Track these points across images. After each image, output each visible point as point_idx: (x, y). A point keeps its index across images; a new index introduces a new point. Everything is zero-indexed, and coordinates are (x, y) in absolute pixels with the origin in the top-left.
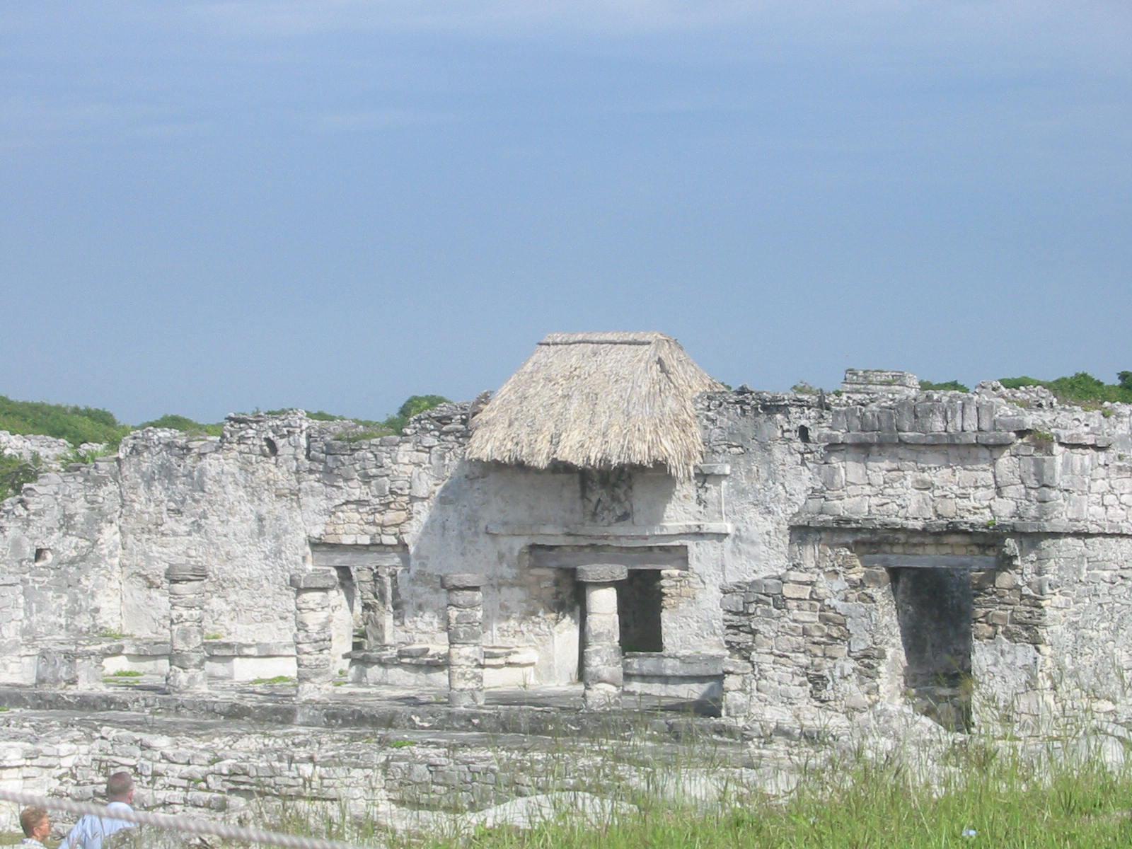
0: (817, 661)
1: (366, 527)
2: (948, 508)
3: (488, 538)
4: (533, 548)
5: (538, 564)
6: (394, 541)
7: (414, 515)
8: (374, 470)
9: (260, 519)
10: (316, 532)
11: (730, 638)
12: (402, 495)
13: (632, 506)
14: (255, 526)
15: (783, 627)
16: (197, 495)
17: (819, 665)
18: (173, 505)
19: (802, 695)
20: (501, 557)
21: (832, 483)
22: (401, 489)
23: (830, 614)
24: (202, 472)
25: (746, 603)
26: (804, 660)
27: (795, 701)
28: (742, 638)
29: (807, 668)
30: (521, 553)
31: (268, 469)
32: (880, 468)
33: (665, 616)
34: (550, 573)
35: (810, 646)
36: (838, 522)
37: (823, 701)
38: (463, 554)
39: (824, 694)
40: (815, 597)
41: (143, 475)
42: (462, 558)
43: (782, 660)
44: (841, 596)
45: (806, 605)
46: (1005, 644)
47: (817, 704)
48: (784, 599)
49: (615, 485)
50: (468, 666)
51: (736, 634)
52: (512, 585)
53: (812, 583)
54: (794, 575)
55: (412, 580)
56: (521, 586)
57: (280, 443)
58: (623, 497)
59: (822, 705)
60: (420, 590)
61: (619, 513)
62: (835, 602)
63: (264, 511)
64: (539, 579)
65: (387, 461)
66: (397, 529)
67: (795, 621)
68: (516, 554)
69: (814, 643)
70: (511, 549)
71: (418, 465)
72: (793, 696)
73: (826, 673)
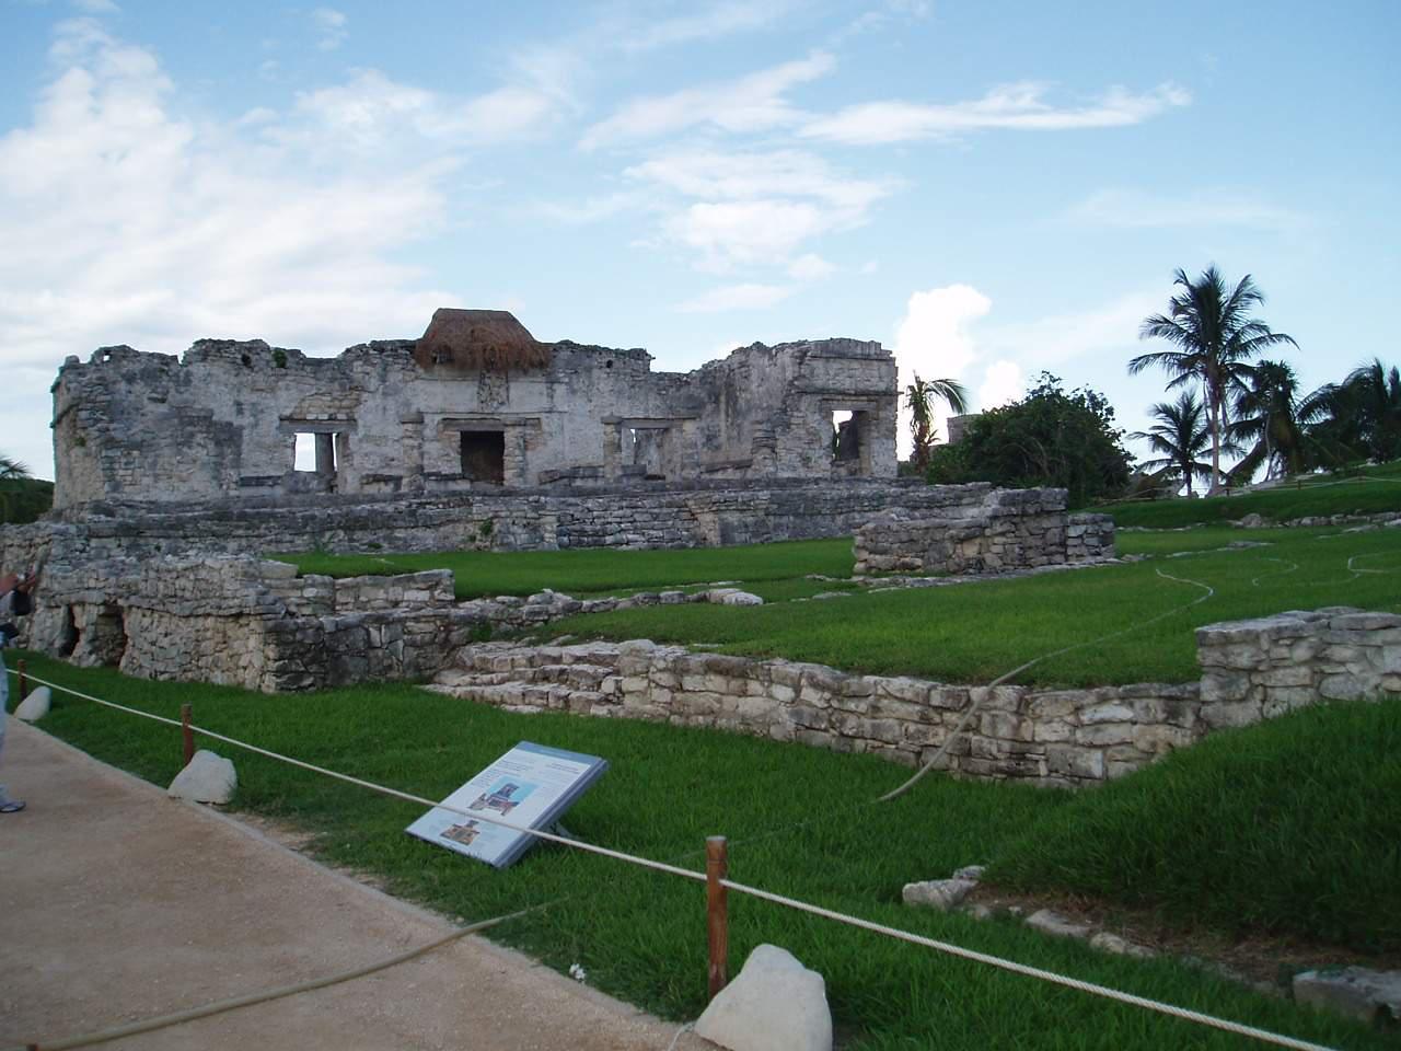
1: (327, 410)
2: (861, 386)
4: (444, 419)
5: (445, 428)
6: (344, 417)
9: (238, 404)
10: (287, 412)
14: (235, 408)
16: (182, 389)
18: (154, 395)
24: (188, 374)
26: (800, 451)
30: (438, 424)
31: (247, 376)
32: (835, 366)
34: (459, 433)
39: (810, 465)
41: (123, 376)
46: (885, 441)
48: (791, 424)
52: (432, 441)
55: (361, 441)
56: (438, 441)
57: (254, 358)
60: (365, 445)
63: (242, 399)
64: (450, 436)
65: (347, 372)
66: (348, 411)
68: (436, 423)
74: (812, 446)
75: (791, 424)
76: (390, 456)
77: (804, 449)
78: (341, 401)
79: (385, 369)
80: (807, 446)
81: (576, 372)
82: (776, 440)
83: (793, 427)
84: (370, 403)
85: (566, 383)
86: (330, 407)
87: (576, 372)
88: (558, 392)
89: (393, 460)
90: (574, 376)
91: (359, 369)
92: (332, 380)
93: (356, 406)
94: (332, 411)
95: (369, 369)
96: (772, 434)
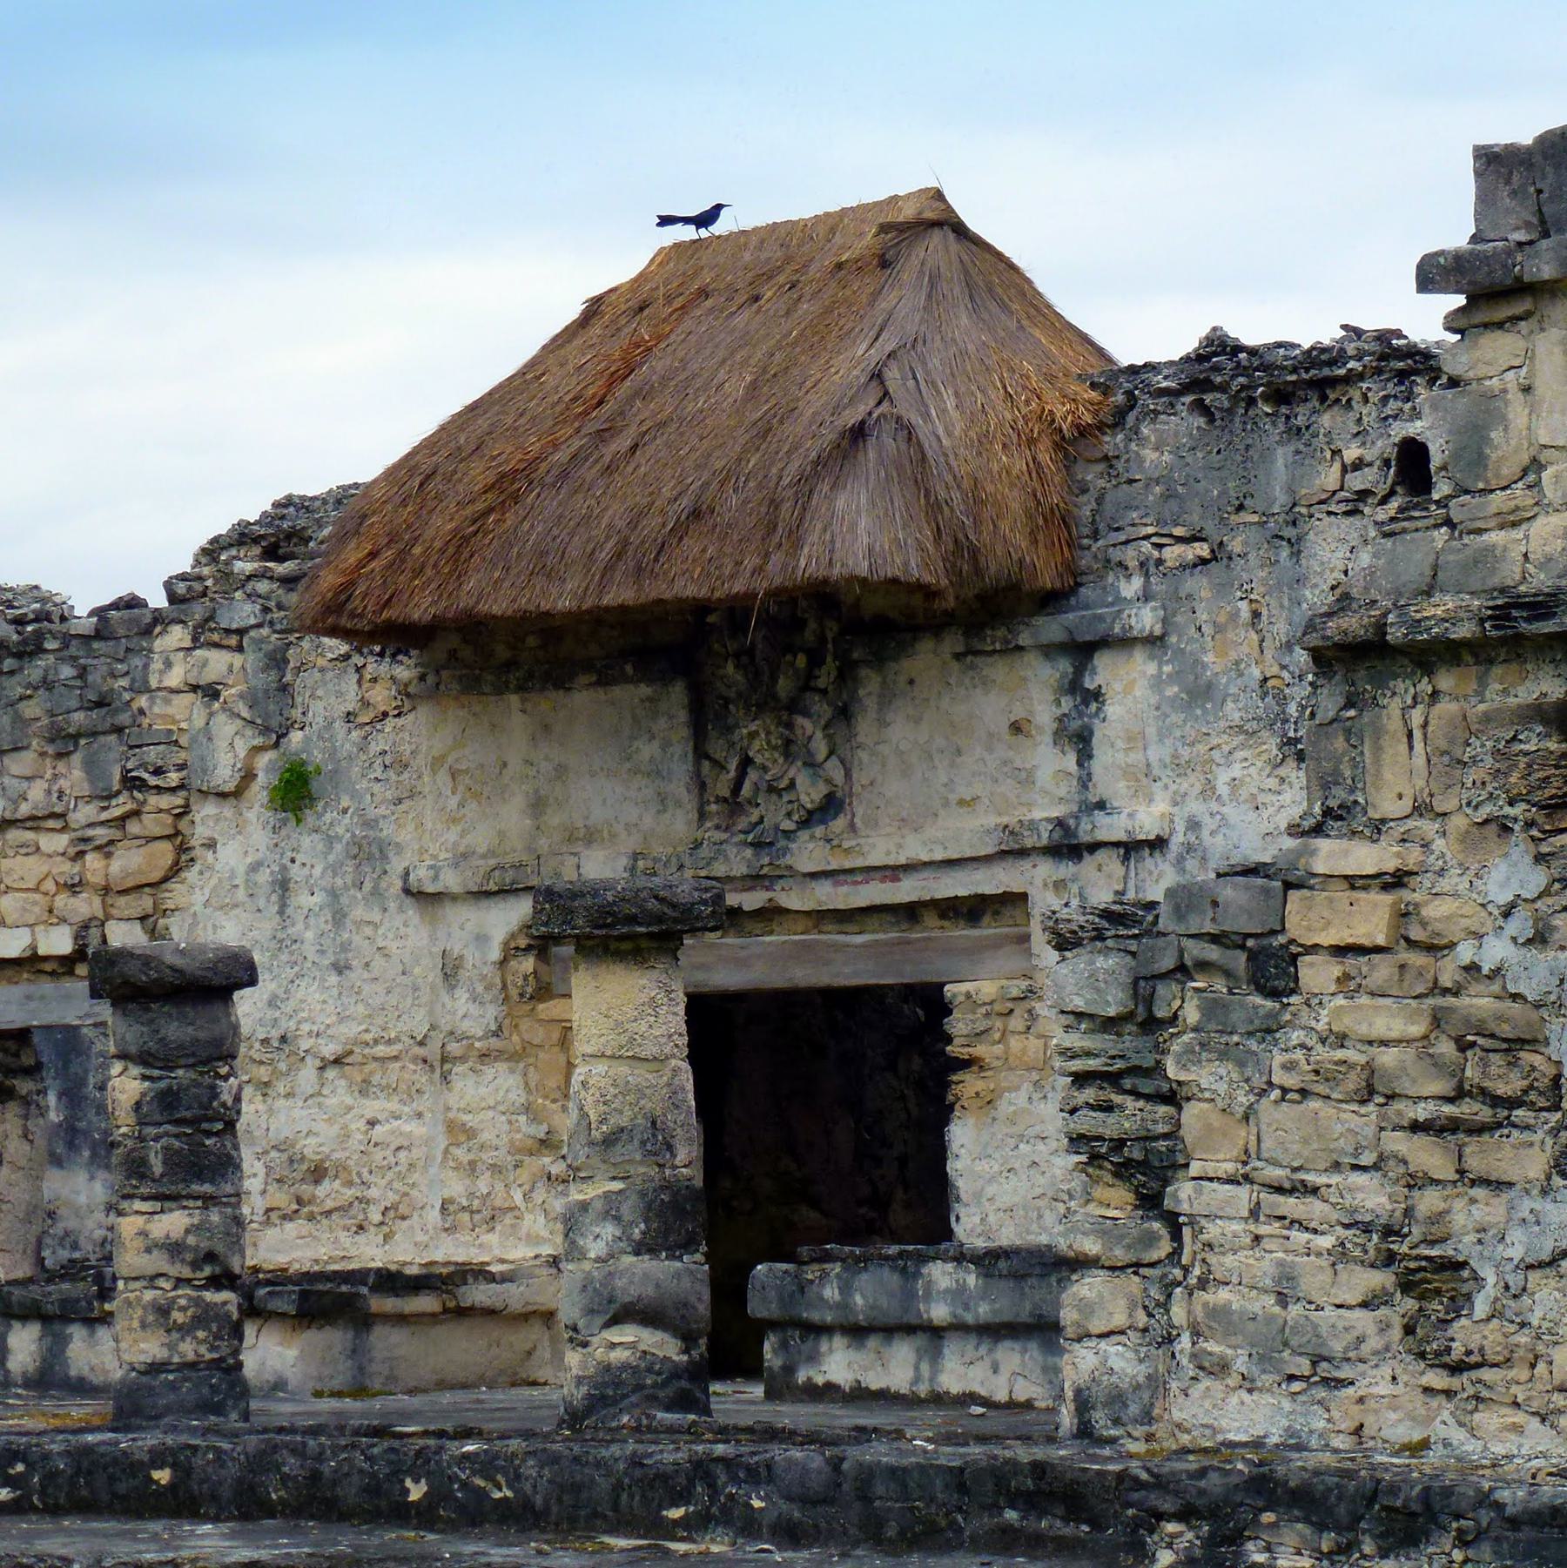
0: (1428, 1201)
1: (62, 901)
3: (412, 912)
7: (198, 852)
8: (79, 717)
11: (1088, 1122)
12: (159, 789)
13: (848, 774)
15: (1289, 1067)
17: (1438, 1217)
19: (1374, 1343)
20: (450, 971)
21: (1480, 461)
22: (158, 772)
23: (1479, 1002)
25: (1143, 985)
27: (1345, 1373)
28: (1131, 1116)
29: (1389, 1232)
33: (962, 1135)
35: (1398, 1143)
36: (1501, 615)
37: (1457, 1369)
38: (340, 968)
39: (1464, 1335)
40: (1416, 933)
42: (333, 979)
43: (1290, 1205)
44: (1520, 925)
45: (1381, 971)
47: (1437, 1379)
49: (795, 706)
50: (179, 1282)
51: (1108, 1108)
52: (484, 1056)
53: (1396, 880)
54: (1332, 855)
56: (513, 1057)
58: (820, 747)
59: (1454, 1383)
61: (810, 793)
62: (1496, 951)
66: (146, 903)
67: (1341, 1040)
68: (495, 954)
69: (1416, 1127)
70: (481, 939)
71: (211, 692)
72: (1337, 1347)
73: (1464, 1246)
74: (1481, 1156)
75: (1290, 958)
76: (310, 1147)
77: (1416, 1181)
78: (106, 849)
79: (277, 661)
80: (1429, 1156)
81: (1219, 554)
82: (1173, 1097)
83: (1317, 974)
84: (231, 857)
85: (1154, 642)
86: (74, 888)
87: (1219, 554)
88: (1113, 710)
89: (318, 1173)
90: (1199, 585)
91: (175, 678)
92: (63, 742)
93: (175, 871)
94: (84, 906)
95: (217, 663)
96: (1129, 1043)
